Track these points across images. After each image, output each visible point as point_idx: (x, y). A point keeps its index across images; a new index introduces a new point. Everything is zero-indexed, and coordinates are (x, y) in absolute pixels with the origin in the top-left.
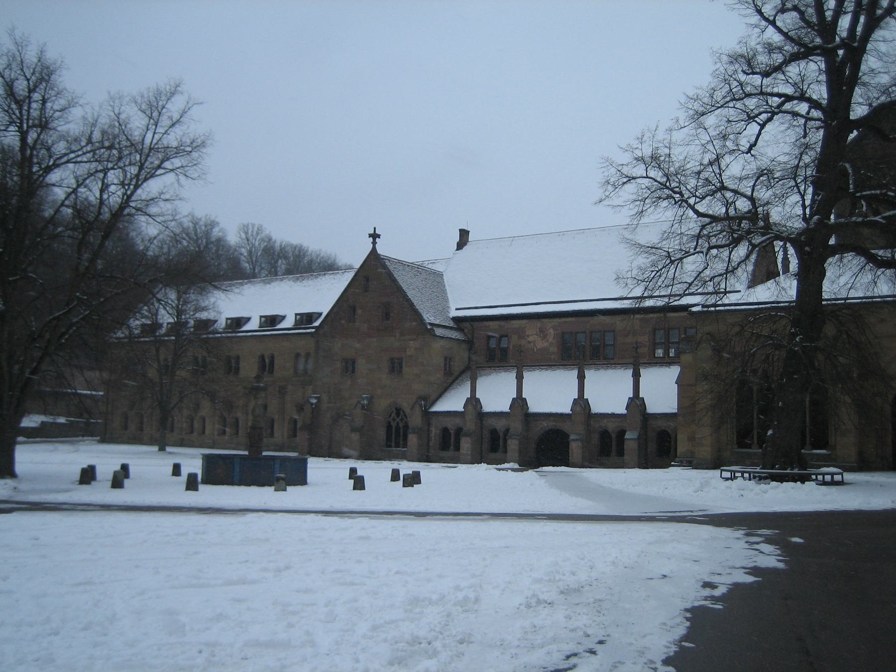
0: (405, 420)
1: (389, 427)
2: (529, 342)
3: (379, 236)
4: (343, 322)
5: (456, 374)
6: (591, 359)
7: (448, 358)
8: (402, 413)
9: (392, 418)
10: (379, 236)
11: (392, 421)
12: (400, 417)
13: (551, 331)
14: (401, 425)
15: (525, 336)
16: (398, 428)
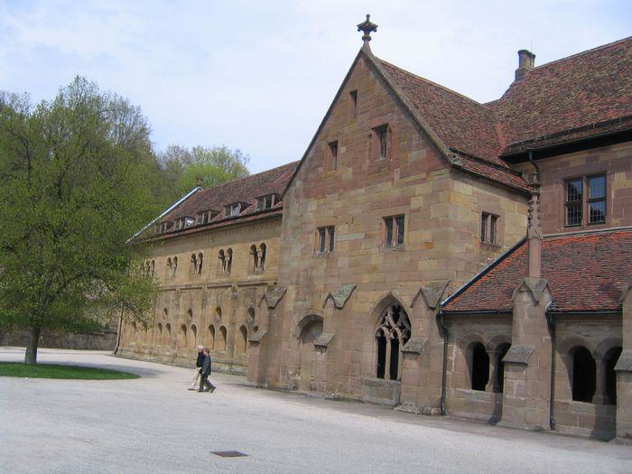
1: (381, 341)
3: (373, 28)
5: (506, 249)
7: (490, 217)
8: (401, 314)
10: (373, 28)
11: (384, 329)
12: (399, 324)
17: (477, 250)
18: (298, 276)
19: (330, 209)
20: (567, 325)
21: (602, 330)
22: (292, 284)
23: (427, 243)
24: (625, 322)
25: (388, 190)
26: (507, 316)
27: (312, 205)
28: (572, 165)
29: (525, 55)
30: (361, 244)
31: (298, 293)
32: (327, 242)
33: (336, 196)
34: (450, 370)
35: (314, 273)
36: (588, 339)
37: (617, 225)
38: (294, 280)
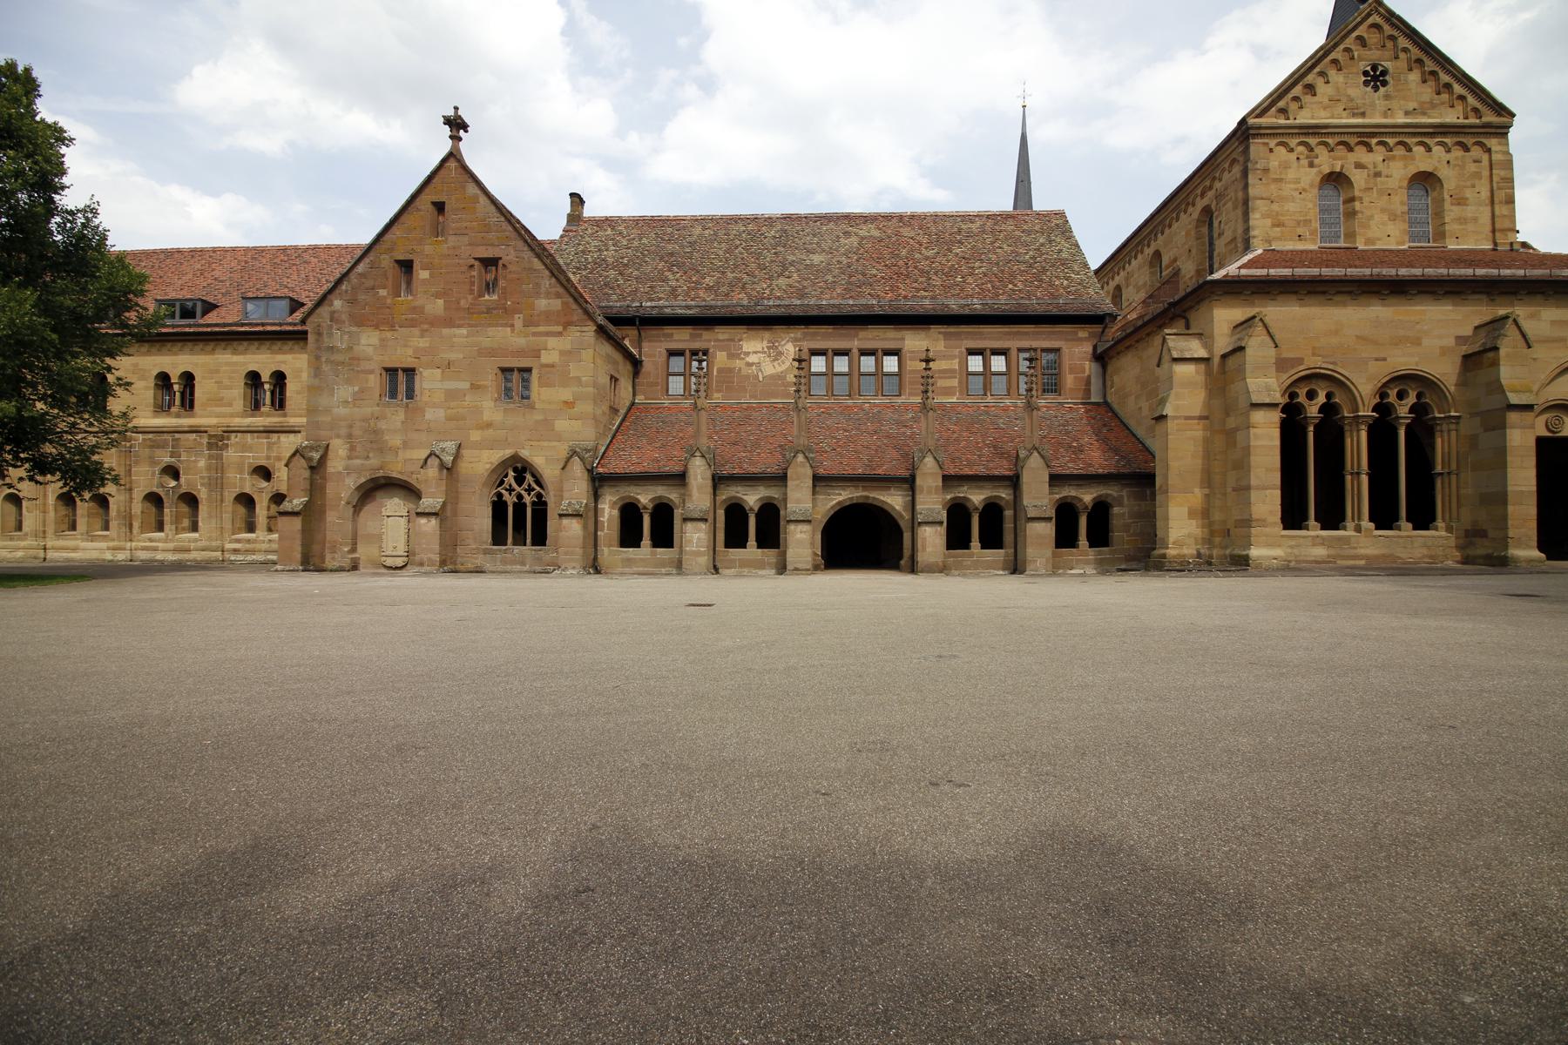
0: (538, 489)
1: (499, 507)
2: (750, 365)
4: (383, 292)
5: (623, 412)
8: (528, 476)
9: (506, 485)
11: (503, 492)
12: (525, 485)
14: (528, 499)
16: (520, 507)
17: (608, 412)
18: (351, 427)
19: (406, 346)
22: (338, 436)
23: (566, 402)
24: (790, 483)
25: (508, 337)
26: (680, 478)
27: (368, 340)
29: (577, 200)
30: (465, 395)
31: (352, 449)
32: (402, 388)
33: (416, 331)
34: (603, 530)
35: (382, 425)
36: (745, 497)
37: (719, 398)
38: (343, 431)
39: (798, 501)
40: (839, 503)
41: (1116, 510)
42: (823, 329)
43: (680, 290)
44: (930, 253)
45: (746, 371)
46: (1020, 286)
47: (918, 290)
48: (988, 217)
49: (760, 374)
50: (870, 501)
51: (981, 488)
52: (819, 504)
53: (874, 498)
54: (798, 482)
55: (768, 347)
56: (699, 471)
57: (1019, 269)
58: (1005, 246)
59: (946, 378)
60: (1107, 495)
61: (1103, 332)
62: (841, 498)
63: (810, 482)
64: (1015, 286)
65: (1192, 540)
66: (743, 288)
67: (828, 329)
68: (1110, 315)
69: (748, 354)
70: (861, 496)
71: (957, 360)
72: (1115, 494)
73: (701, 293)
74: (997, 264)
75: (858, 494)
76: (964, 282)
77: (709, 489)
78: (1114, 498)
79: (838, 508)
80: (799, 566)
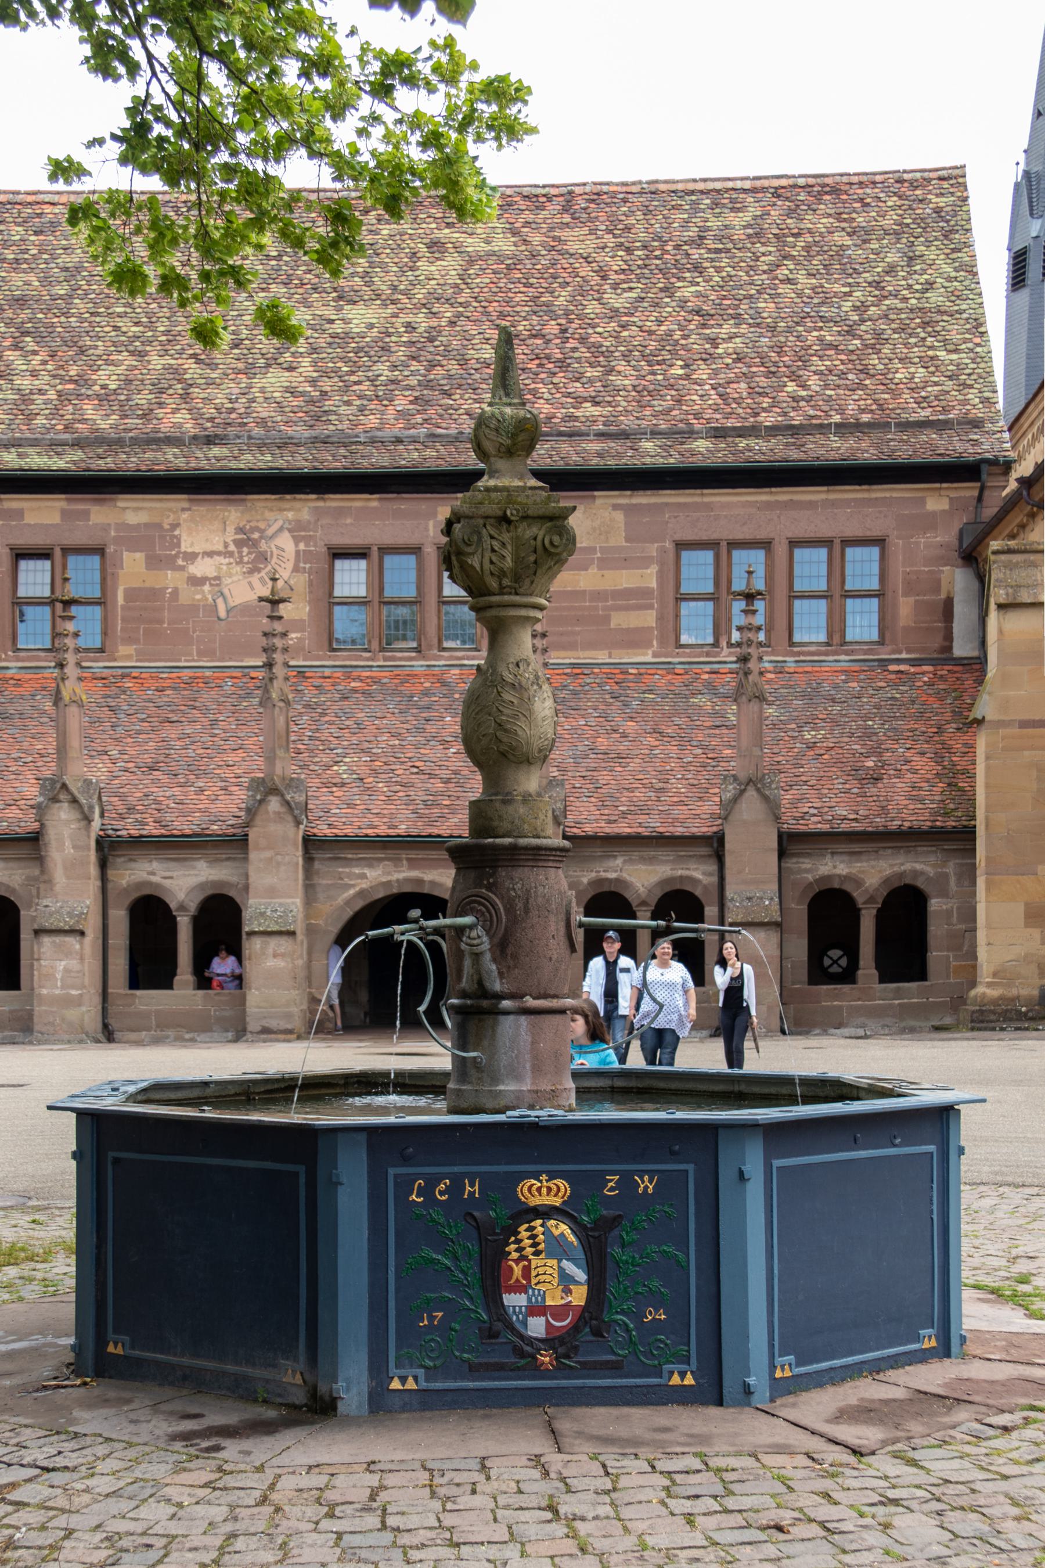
2: (197, 582)
6: (382, 650)
13: (286, 543)
15: (176, 556)
20: (131, 860)
21: (194, 868)
24: (253, 855)
28: (30, 519)
36: (167, 883)
37: (128, 657)
39: (272, 892)
40: (361, 893)
41: (935, 904)
42: (358, 502)
43: (39, 399)
44: (619, 301)
45: (188, 595)
46: (814, 383)
47: (579, 400)
48: (777, 193)
49: (220, 602)
50: (426, 890)
51: (651, 860)
52: (321, 896)
53: (433, 883)
54: (268, 854)
55: (239, 543)
56: (66, 833)
57: (821, 339)
58: (801, 277)
59: (627, 608)
60: (916, 873)
61: (980, 499)
62: (364, 885)
63: (298, 855)
64: (804, 386)
65: (1034, 967)
66: (186, 397)
67: (372, 502)
68: (993, 462)
69: (192, 557)
70: (407, 880)
71: (653, 569)
72: (930, 871)
73: (89, 410)
74: (773, 329)
75: (401, 876)
76: (687, 377)
77: (93, 870)
78: (929, 879)
79: (360, 904)
80: (273, 1024)
